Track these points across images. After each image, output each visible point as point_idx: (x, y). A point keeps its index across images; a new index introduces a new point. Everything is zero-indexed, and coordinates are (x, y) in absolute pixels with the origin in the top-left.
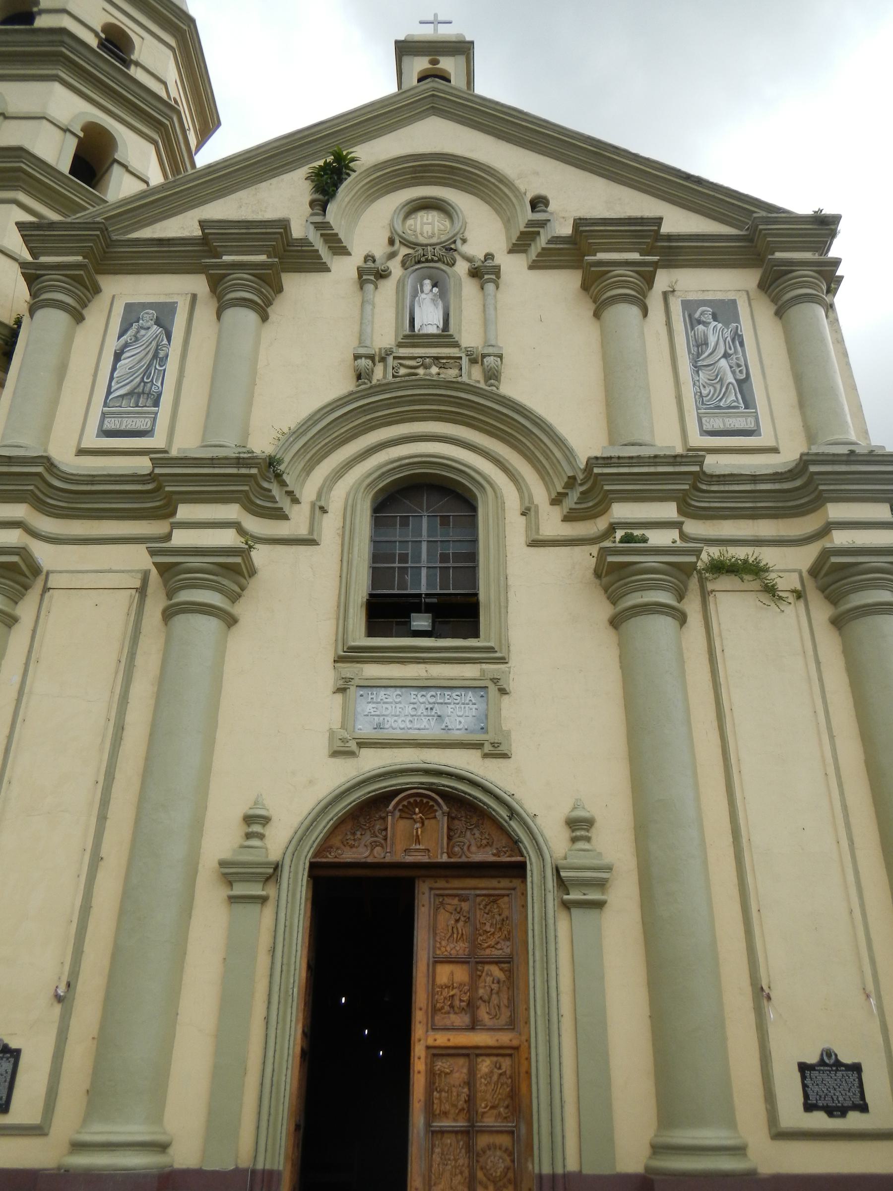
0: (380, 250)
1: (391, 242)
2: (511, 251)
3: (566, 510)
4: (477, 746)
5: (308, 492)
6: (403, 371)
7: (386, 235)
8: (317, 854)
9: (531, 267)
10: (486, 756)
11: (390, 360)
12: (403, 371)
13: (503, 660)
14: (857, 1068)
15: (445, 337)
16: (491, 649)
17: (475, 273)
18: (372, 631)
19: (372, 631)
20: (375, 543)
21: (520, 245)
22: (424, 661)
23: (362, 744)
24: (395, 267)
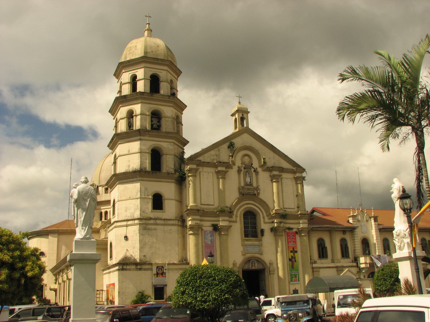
0: (240, 165)
1: (242, 164)
2: (259, 167)
3: (269, 218)
4: (259, 253)
5: (235, 213)
6: (246, 191)
7: (241, 162)
8: (242, 268)
9: (262, 171)
10: (260, 255)
11: (244, 189)
12: (246, 191)
13: (262, 241)
14: (298, 290)
15: (251, 184)
16: (260, 240)
17: (255, 171)
18: (245, 237)
19: (245, 237)
20: (244, 222)
21: (261, 166)
22: (252, 241)
23: (246, 253)
24: (243, 169)
